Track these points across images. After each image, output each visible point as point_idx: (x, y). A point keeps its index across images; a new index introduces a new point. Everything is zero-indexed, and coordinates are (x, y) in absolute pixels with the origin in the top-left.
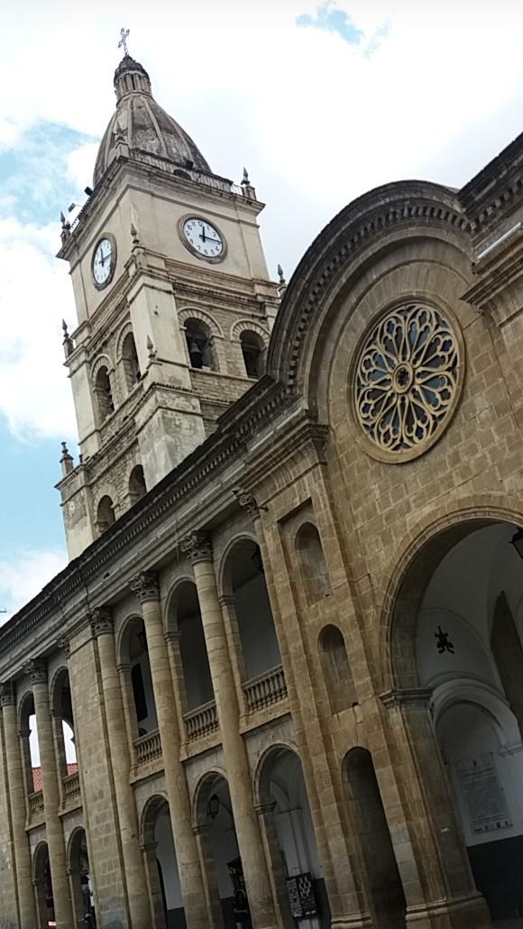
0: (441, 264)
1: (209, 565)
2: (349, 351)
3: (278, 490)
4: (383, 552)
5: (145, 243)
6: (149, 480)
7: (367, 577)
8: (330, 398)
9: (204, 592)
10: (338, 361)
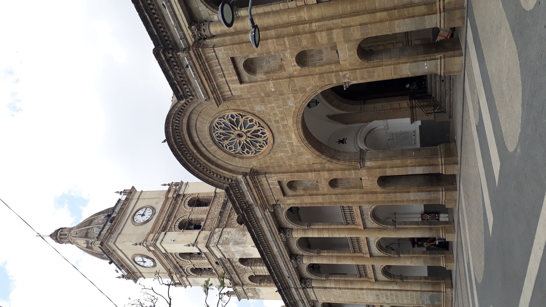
1: (294, 230)
2: (223, 154)
4: (305, 156)
5: (141, 240)
6: (247, 256)
8: (240, 166)
9: (304, 234)
10: (226, 160)
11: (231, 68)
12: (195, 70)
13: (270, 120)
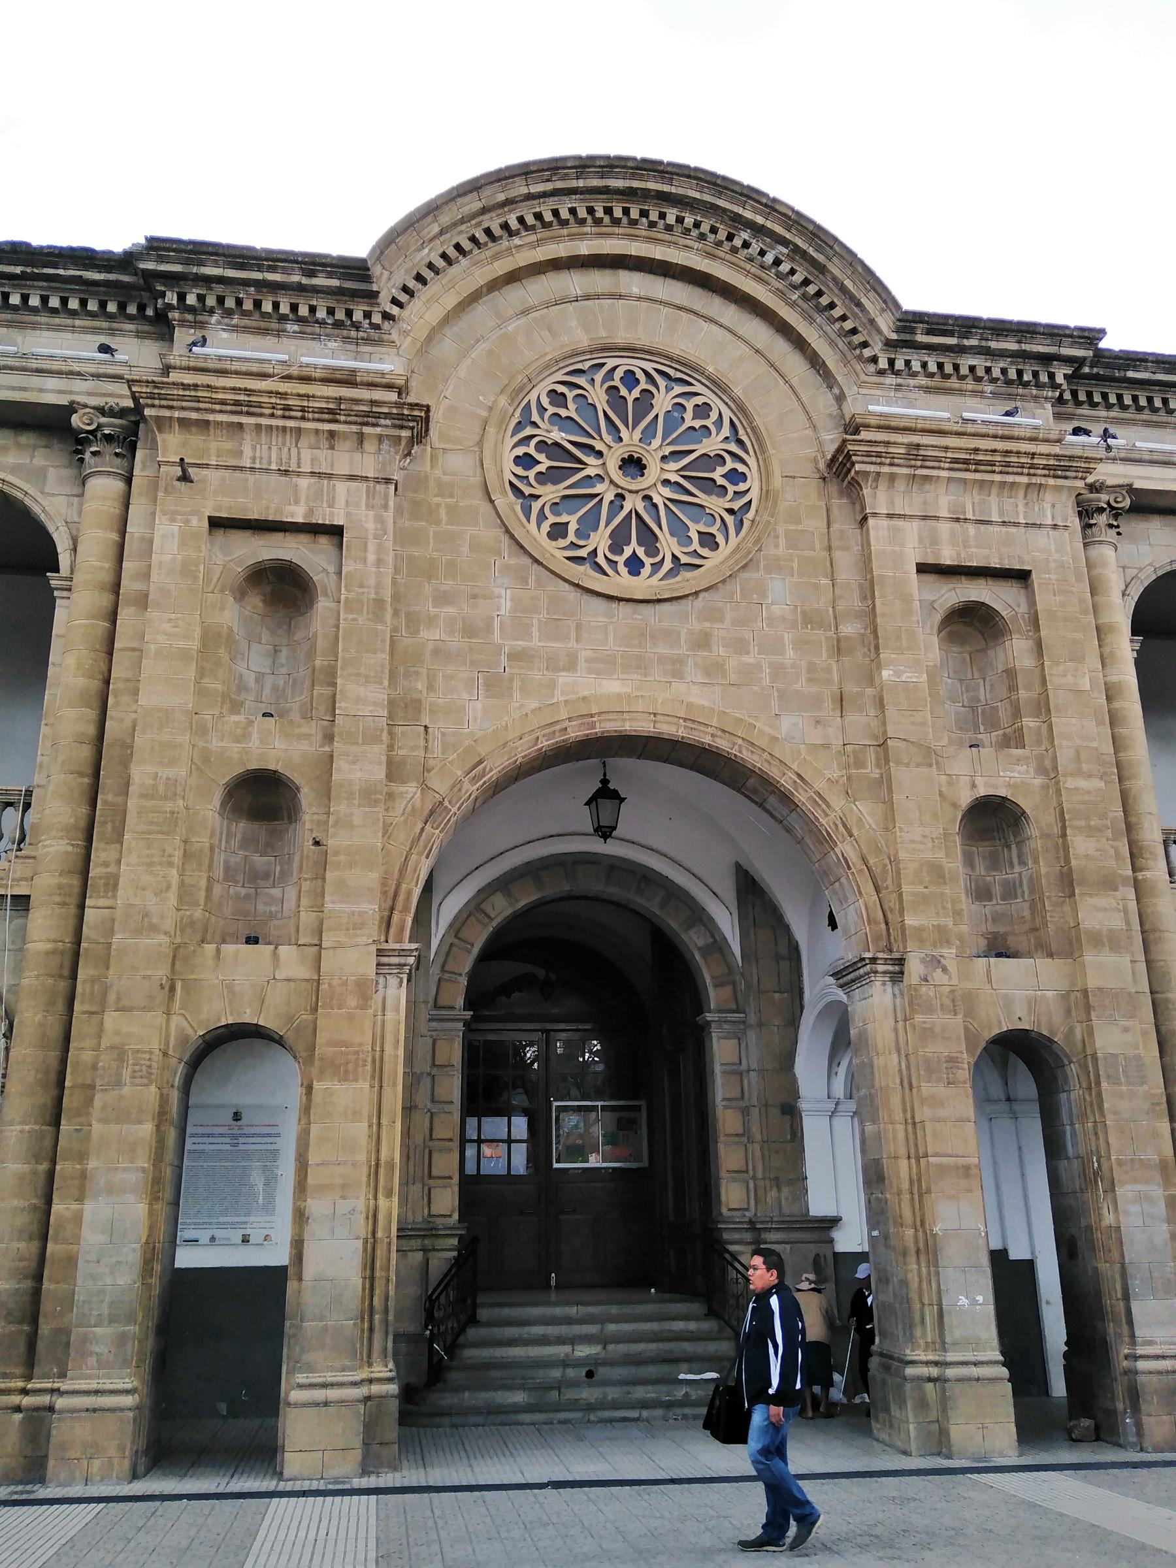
4: (479, 705)
7: (423, 728)
10: (490, 352)
11: (988, 557)
12: (991, 430)
13: (715, 615)
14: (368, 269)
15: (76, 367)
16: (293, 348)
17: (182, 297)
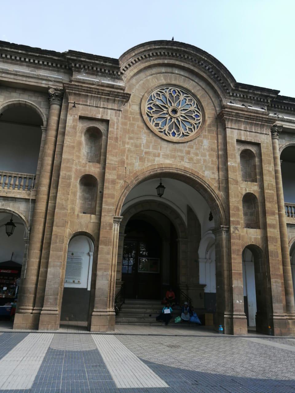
0: (206, 92)
2: (152, 84)
3: (89, 104)
4: (138, 164)
7: (125, 168)
10: (143, 83)
11: (252, 139)
12: (254, 111)
13: (191, 147)
14: (119, 62)
15: (50, 79)
16: (100, 79)
17: (75, 65)
